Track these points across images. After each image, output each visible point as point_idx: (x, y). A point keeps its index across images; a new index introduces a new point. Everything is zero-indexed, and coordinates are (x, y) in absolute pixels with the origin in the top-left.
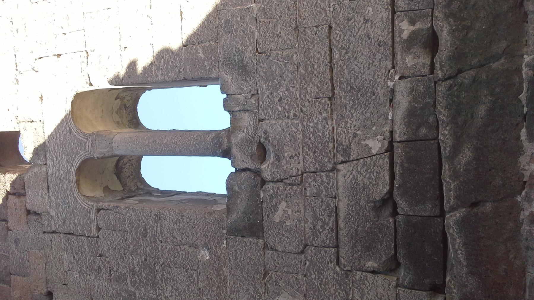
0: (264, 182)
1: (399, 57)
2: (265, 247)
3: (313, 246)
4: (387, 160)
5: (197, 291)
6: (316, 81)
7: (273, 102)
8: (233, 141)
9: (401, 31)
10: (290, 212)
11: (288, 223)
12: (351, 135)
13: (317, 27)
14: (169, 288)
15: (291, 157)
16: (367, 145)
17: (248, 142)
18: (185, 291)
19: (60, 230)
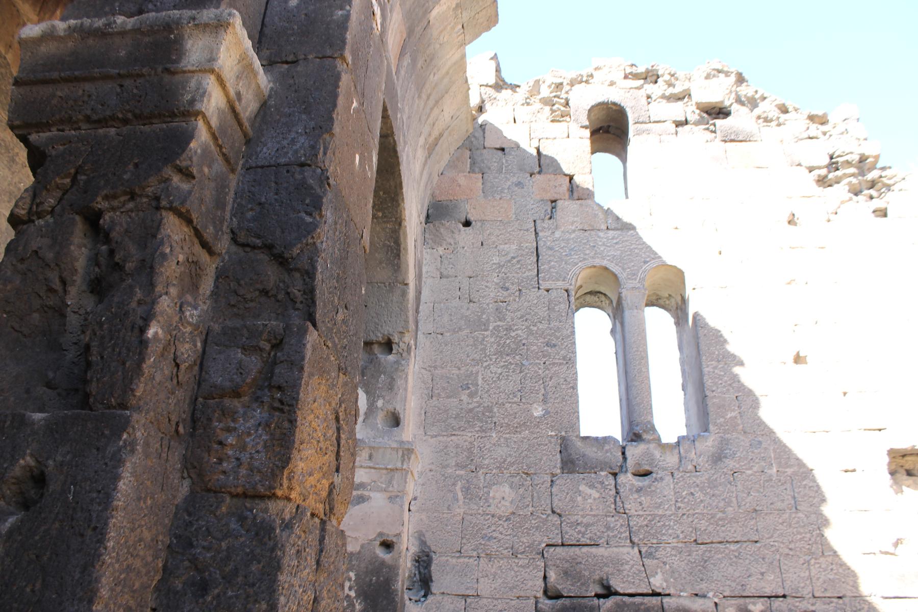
1: (733, 602)
2: (553, 475)
4: (645, 591)
5: (501, 401)
6: (710, 528)
7: (690, 487)
8: (652, 446)
9: (754, 604)
10: (589, 501)
11: (579, 498)
12: (665, 560)
13: (757, 530)
14: (499, 371)
15: (641, 503)
16: (657, 573)
17: (652, 461)
18: (499, 388)
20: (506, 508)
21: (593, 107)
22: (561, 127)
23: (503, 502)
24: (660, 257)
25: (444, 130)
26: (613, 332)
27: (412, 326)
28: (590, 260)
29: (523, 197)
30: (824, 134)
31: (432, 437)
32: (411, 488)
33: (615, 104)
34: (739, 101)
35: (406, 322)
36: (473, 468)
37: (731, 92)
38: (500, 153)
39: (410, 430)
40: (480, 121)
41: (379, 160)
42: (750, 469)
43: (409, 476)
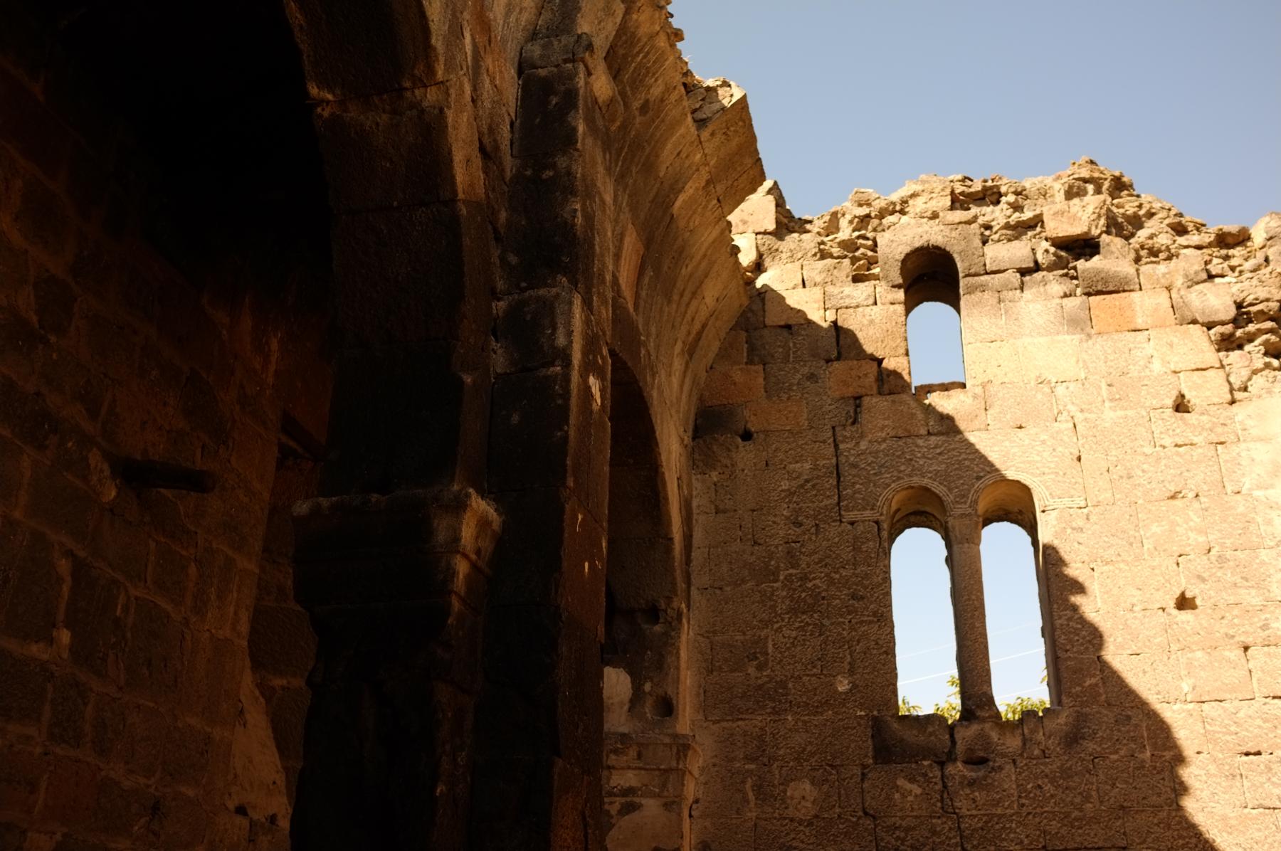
0: (942, 764)
2: (864, 767)
3: (876, 826)
6: (1063, 831)
7: (1037, 778)
8: (987, 726)
10: (910, 798)
11: (897, 796)
13: (1124, 834)
14: (794, 634)
15: (974, 800)
18: (794, 656)
19: (843, 459)
20: (807, 809)
21: (907, 255)
22: (864, 289)
23: (803, 803)
24: (997, 470)
25: (707, 320)
26: (950, 561)
27: (681, 585)
28: (906, 479)
29: (818, 394)
30: (1233, 269)
31: (714, 722)
32: (691, 789)
33: (937, 248)
34: (1115, 226)
35: (674, 584)
36: (765, 760)
37: (1099, 216)
38: (785, 333)
39: (686, 719)
40: (759, 283)
41: (609, 542)
42: (1116, 752)
43: (687, 777)
